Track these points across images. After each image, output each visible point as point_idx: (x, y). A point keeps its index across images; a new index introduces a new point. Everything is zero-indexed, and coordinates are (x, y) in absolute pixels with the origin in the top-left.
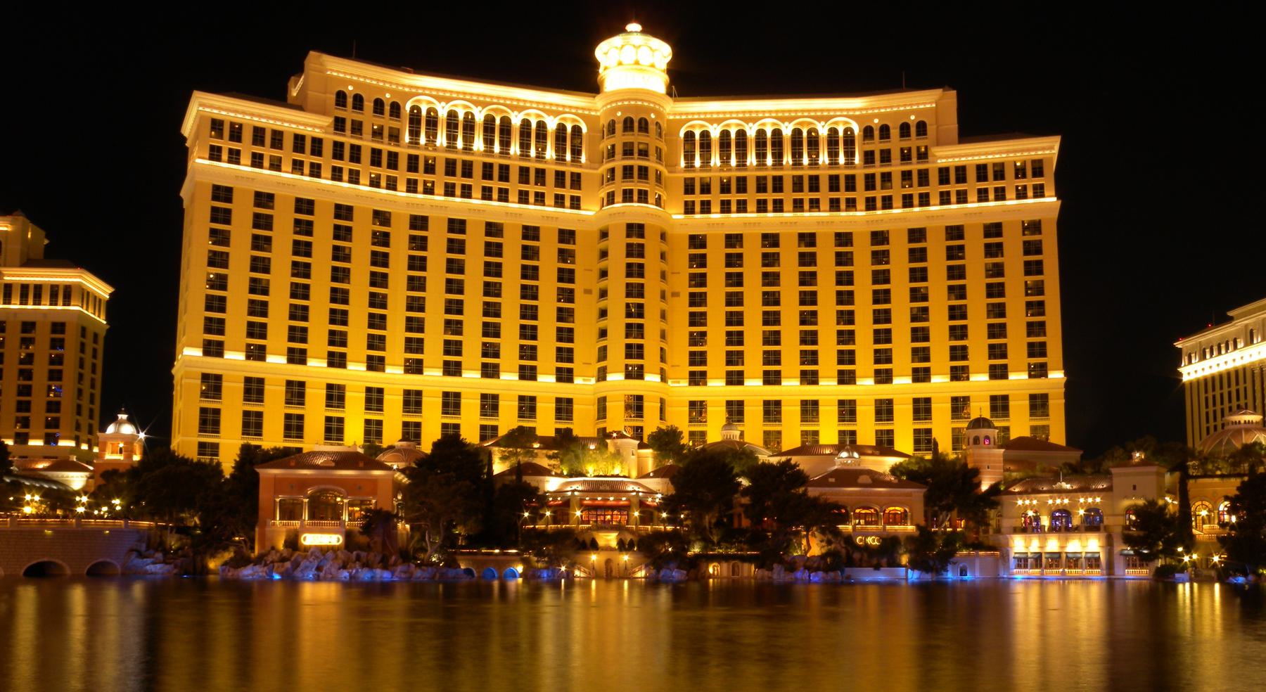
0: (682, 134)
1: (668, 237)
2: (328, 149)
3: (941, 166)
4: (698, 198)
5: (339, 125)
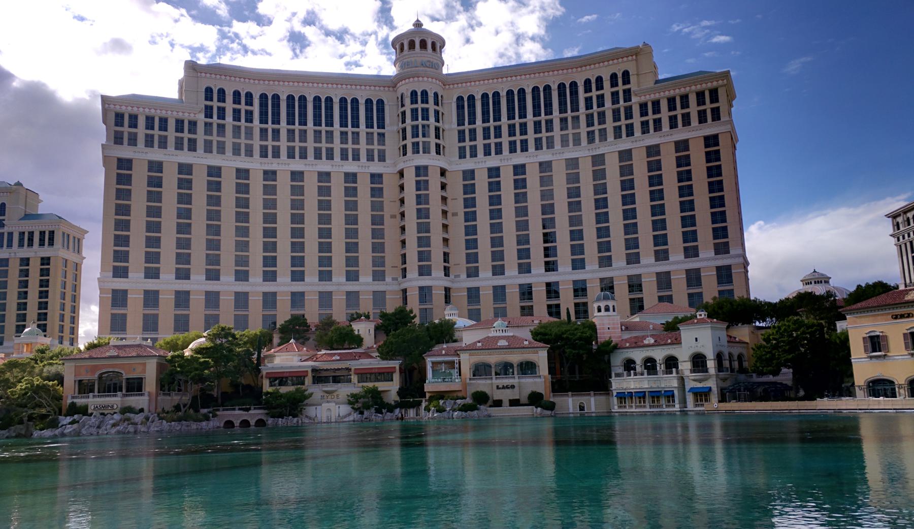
1: (447, 174)
2: (201, 128)
4: (468, 144)
5: (208, 112)
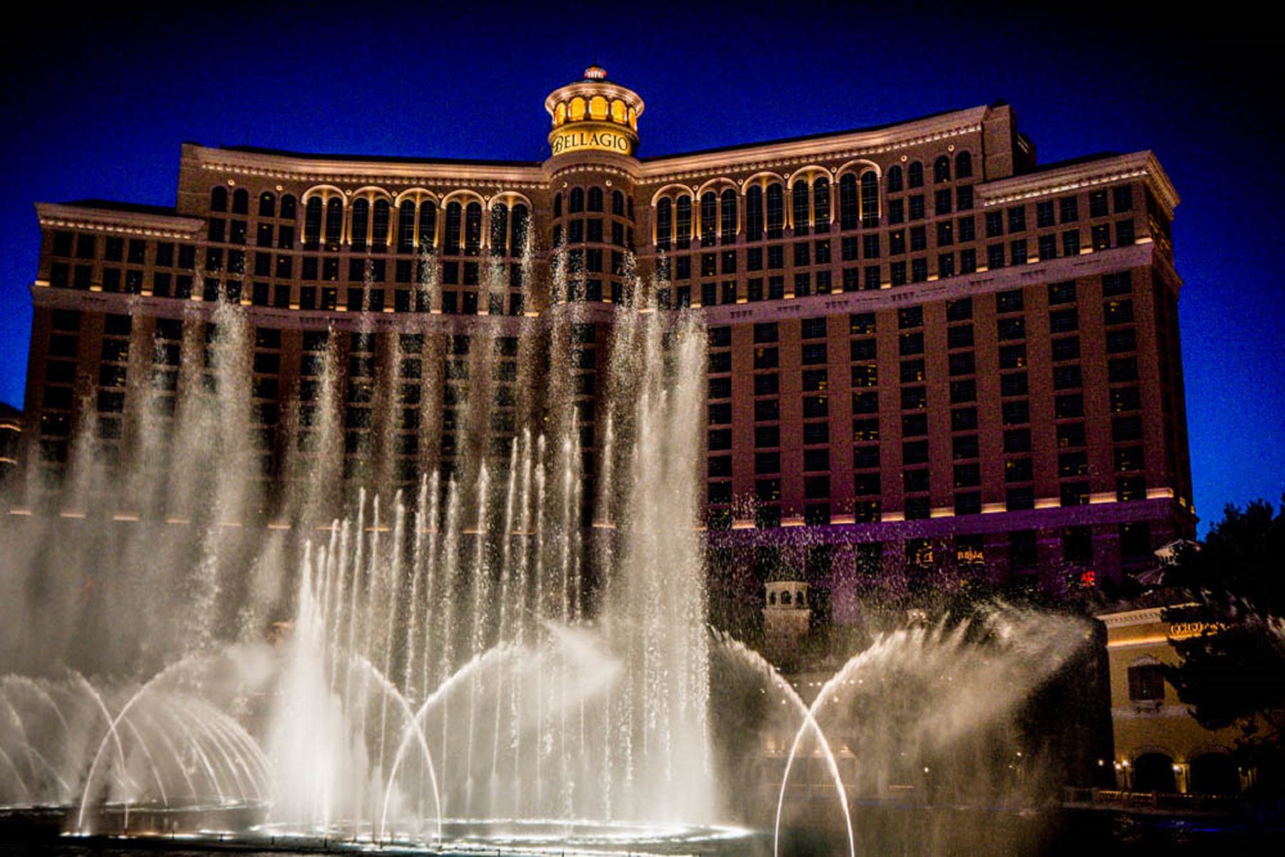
0: (654, 204)
3: (989, 210)
5: (215, 230)
